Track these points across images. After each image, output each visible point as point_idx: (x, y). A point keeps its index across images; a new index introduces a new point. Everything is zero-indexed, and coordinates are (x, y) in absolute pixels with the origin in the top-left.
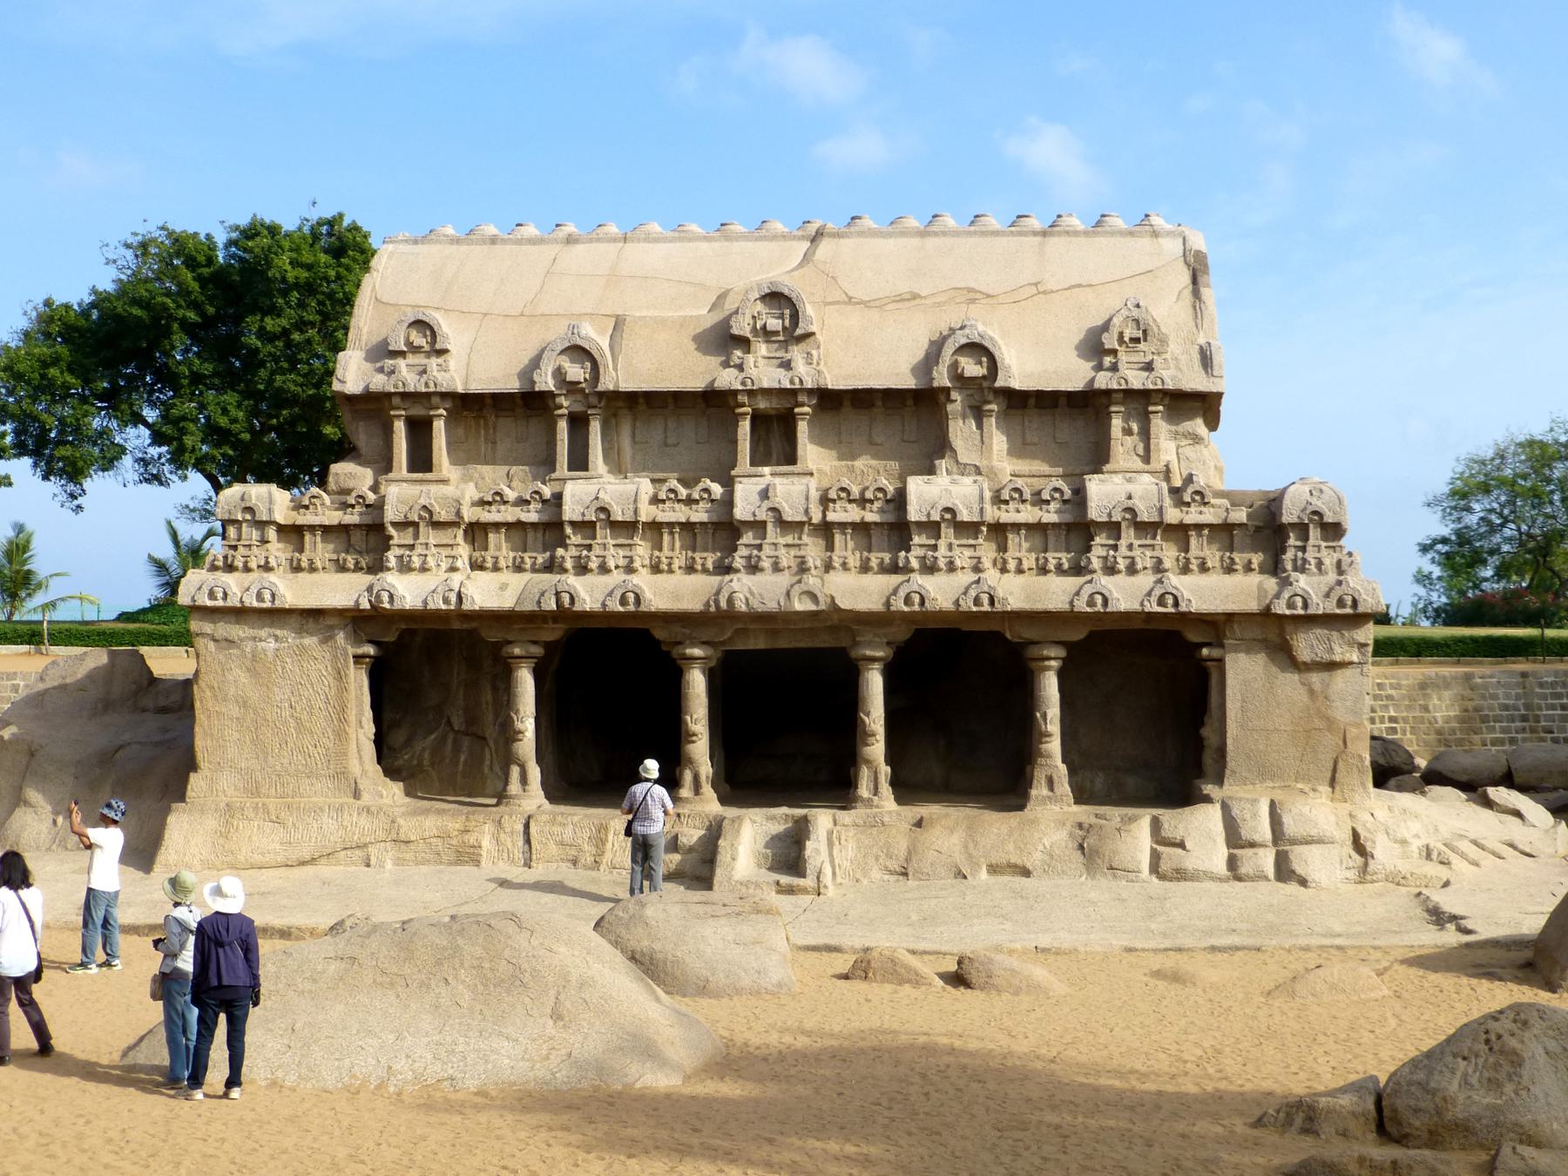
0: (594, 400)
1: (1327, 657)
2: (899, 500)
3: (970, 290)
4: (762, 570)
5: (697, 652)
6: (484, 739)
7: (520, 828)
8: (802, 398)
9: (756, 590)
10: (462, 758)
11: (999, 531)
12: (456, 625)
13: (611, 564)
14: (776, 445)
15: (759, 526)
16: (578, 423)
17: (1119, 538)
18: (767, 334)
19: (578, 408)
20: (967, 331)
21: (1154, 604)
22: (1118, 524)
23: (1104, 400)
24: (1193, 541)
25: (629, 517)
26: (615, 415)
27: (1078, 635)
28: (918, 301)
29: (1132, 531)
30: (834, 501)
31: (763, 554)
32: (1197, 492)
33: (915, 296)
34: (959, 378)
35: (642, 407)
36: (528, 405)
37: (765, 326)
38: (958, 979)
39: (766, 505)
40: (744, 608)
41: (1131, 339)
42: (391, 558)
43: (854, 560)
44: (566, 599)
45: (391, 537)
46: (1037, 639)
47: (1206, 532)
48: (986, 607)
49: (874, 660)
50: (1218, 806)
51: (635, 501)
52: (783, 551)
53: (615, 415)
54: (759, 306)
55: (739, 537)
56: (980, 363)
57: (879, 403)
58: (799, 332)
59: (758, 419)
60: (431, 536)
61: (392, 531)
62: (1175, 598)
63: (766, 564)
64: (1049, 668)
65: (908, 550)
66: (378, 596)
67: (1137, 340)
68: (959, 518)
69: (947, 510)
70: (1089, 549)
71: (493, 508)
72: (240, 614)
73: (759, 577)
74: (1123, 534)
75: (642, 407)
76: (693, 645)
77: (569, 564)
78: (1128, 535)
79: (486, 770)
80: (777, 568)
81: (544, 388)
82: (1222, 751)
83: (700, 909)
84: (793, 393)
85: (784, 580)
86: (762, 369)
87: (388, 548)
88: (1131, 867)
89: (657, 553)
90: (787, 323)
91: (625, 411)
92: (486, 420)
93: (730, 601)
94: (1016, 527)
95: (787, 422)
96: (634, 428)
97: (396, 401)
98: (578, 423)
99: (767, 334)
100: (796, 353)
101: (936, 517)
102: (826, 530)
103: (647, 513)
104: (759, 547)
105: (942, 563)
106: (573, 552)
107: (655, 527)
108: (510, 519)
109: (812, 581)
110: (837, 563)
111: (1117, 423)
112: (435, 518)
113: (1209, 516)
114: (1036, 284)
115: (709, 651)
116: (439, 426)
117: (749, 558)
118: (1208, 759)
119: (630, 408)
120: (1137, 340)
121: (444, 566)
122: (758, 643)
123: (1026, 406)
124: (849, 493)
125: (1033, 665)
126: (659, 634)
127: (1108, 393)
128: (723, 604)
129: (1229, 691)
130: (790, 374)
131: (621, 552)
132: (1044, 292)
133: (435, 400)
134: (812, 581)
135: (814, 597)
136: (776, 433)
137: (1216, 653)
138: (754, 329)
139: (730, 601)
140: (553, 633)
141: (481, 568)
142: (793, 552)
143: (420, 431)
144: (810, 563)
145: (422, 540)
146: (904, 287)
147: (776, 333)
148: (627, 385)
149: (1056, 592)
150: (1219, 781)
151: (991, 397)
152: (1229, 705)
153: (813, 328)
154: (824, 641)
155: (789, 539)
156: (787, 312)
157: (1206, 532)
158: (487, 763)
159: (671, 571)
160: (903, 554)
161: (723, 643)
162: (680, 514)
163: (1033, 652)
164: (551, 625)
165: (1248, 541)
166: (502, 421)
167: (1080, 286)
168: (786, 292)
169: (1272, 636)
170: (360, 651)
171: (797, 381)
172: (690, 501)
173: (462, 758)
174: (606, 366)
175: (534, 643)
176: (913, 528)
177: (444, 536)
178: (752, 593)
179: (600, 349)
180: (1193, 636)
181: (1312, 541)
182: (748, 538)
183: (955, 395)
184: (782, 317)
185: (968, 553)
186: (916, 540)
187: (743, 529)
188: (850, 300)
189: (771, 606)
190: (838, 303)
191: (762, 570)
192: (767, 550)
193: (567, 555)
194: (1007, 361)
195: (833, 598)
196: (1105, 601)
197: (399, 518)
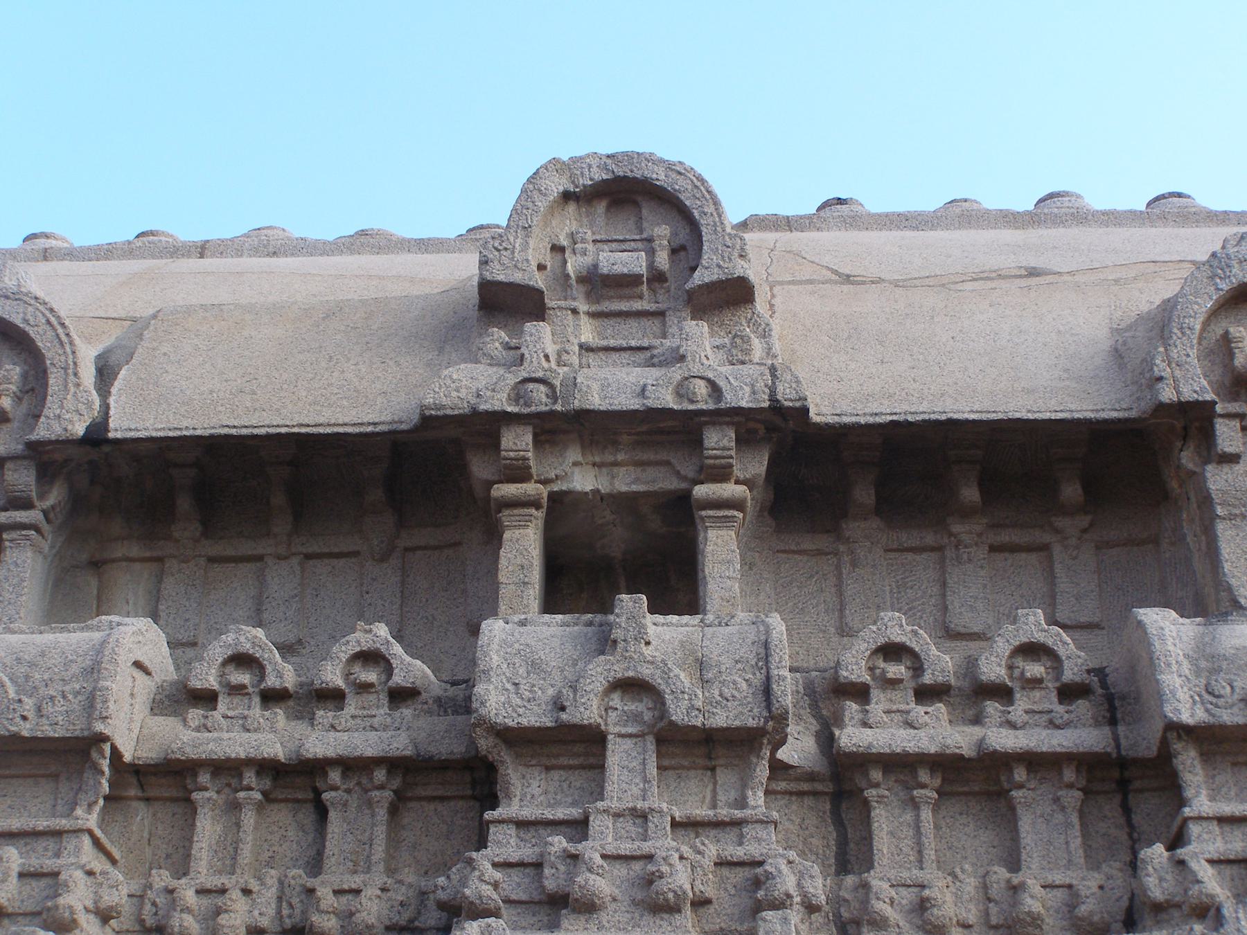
2: (1114, 693)
4: (588, 907)
8: (719, 440)
15: (571, 746)
26: (97, 565)
30: (860, 693)
31: (591, 850)
33: (1033, 273)
52: (663, 843)
57: (970, 494)
58: (701, 277)
65: (1177, 841)
89: (162, 878)
90: (663, 260)
102: (842, 788)
103: (134, 729)
104: (579, 827)
107: (166, 783)
124: (918, 668)
130: (676, 373)
136: (626, 558)
168: (660, 176)
171: (701, 388)
182: (528, 793)
191: (588, 907)
192: (607, 835)
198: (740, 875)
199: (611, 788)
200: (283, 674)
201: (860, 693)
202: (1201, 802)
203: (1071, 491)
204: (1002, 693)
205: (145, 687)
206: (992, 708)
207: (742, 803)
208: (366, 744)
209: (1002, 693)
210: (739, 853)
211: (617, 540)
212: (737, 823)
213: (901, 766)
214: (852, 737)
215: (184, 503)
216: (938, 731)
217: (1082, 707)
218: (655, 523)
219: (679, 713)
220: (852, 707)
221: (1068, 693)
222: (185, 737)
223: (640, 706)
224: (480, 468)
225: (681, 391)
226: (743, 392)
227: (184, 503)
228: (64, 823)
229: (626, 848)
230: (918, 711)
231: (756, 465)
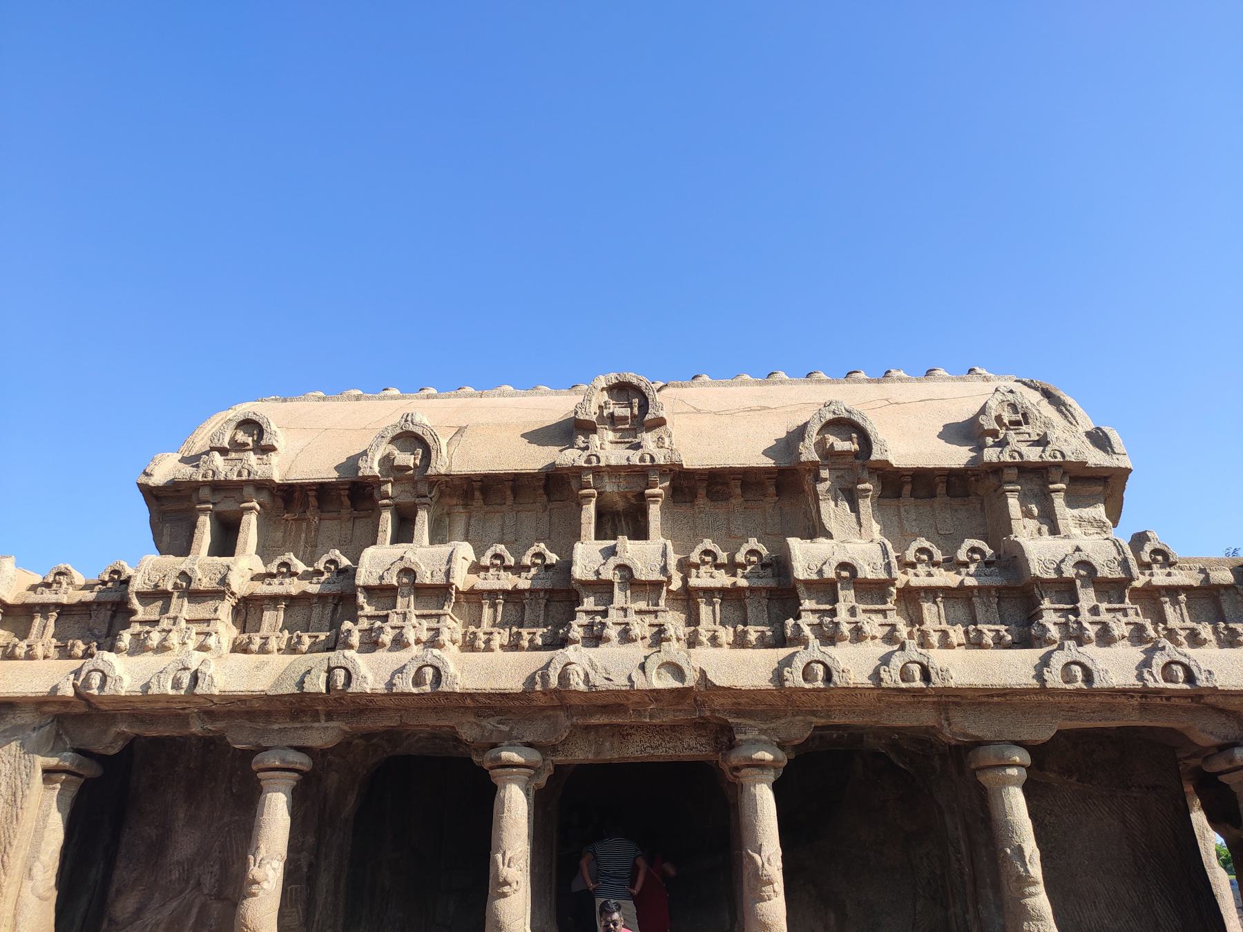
0: (424, 489)
2: (780, 565)
4: (608, 640)
9: (604, 664)
11: (911, 598)
12: (196, 728)
13: (410, 636)
15: (602, 589)
18: (613, 420)
19: (406, 499)
20: (832, 407)
21: (1159, 678)
22: (1070, 583)
23: (993, 480)
25: (439, 579)
27: (1043, 733)
29: (1091, 592)
30: (697, 567)
31: (608, 621)
32: (1156, 552)
33: (764, 408)
34: (829, 455)
37: (612, 414)
39: (613, 561)
40: (582, 687)
41: (1012, 423)
42: (126, 638)
43: (726, 635)
44: (340, 676)
45: (134, 612)
46: (988, 735)
47: (1182, 597)
48: (918, 684)
49: (761, 765)
51: (449, 561)
52: (633, 618)
54: (605, 396)
55: (579, 602)
56: (851, 439)
60: (184, 609)
61: (135, 603)
62: (1187, 669)
63: (612, 632)
64: (1009, 781)
65: (798, 617)
67: (1018, 423)
68: (860, 575)
69: (843, 566)
71: (276, 581)
73: (603, 648)
76: (511, 747)
77: (355, 639)
80: (626, 637)
81: (368, 473)
85: (638, 651)
86: (608, 449)
87: (127, 625)
89: (472, 629)
90: (636, 411)
93: (564, 677)
94: (932, 592)
96: (468, 525)
97: (205, 493)
99: (613, 420)
100: (648, 440)
101: (830, 573)
103: (462, 579)
104: (605, 614)
105: (845, 629)
106: (364, 623)
107: (474, 597)
108: (294, 591)
109: (674, 650)
110: (704, 637)
111: (1013, 503)
112: (193, 586)
113: (1180, 578)
115: (535, 756)
117: (589, 627)
119: (465, 505)
120: (1018, 423)
121: (191, 644)
124: (715, 557)
125: (986, 778)
126: (468, 732)
128: (554, 682)
130: (640, 452)
131: (425, 623)
133: (248, 491)
134: (674, 650)
135: (677, 671)
138: (601, 416)
139: (564, 677)
140: (323, 735)
141: (245, 651)
142: (649, 619)
144: (671, 632)
145: (172, 613)
147: (623, 419)
148: (461, 466)
149: (1011, 668)
151: (865, 475)
153: (663, 414)
154: (691, 748)
155: (642, 605)
156: (636, 401)
157: (1182, 597)
159: (488, 649)
160: (791, 621)
161: (554, 749)
162: (508, 581)
163: (987, 755)
164: (323, 724)
166: (327, 523)
170: (53, 761)
171: (648, 458)
172: (518, 569)
174: (439, 451)
175: (299, 749)
176: (801, 590)
177: (202, 610)
178: (592, 665)
182: (589, 603)
183: (825, 473)
184: (631, 406)
185: (878, 619)
186: (807, 604)
187: (582, 593)
188: (699, 411)
189: (620, 682)
191: (608, 640)
192: (614, 615)
193: (354, 631)
194: (880, 437)
195: (703, 673)
197: (148, 588)
198: (656, 629)
199: (616, 600)
200: (510, 561)
205: (467, 565)
207: (657, 605)
210: (656, 622)
211: (621, 505)
212: (655, 612)
214: (694, 582)
215: (477, 494)
217: (769, 571)
218: (633, 501)
220: (694, 571)
222: (480, 582)
223: (626, 573)
225: (642, 459)
227: (477, 494)
228: (441, 612)
230: (716, 572)
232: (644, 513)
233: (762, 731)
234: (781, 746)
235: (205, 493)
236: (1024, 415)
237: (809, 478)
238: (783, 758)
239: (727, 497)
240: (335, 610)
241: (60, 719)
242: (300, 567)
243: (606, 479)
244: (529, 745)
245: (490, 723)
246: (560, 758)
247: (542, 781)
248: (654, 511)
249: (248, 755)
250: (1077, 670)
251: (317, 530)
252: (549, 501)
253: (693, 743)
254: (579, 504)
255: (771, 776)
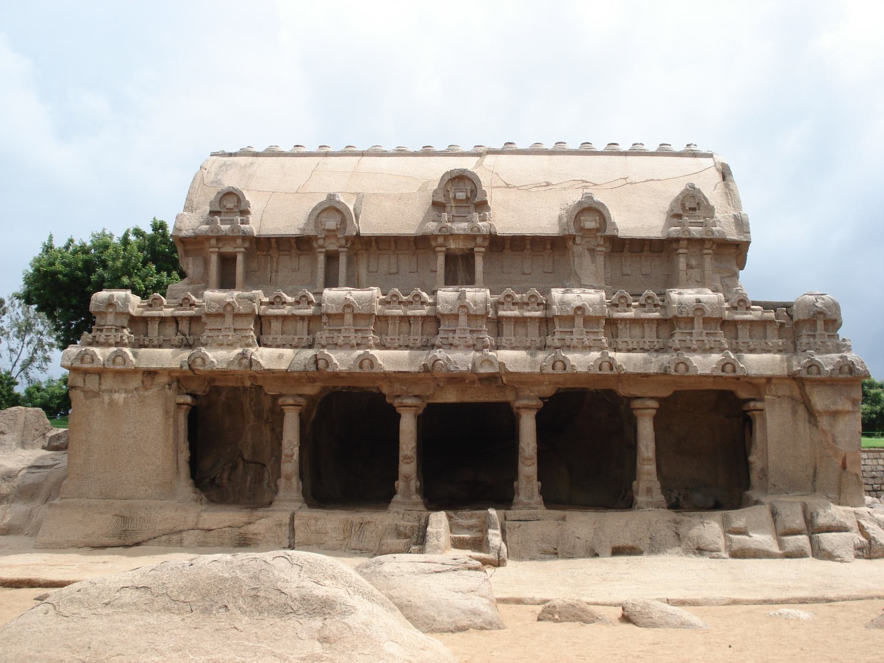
0: (343, 242)
1: (833, 408)
3: (583, 181)
5: (409, 401)
6: (264, 466)
7: (287, 520)
8: (479, 241)
10: (249, 478)
14: (461, 274)
16: (332, 258)
17: (693, 328)
23: (675, 246)
24: (740, 333)
26: (356, 254)
27: (665, 393)
28: (550, 187)
29: (701, 325)
30: (503, 304)
33: (548, 184)
35: (374, 248)
36: (301, 244)
38: (626, 619)
41: (690, 209)
44: (321, 364)
45: (205, 324)
46: (639, 394)
50: (768, 506)
53: (356, 254)
57: (528, 247)
58: (477, 200)
59: (450, 258)
62: (734, 366)
66: (194, 362)
67: (694, 209)
68: (587, 314)
70: (672, 335)
72: (100, 373)
74: (696, 326)
75: (374, 248)
76: (408, 397)
78: (698, 325)
79: (265, 486)
82: (764, 472)
83: (426, 566)
84: (474, 237)
88: (711, 547)
90: (469, 194)
91: (363, 252)
92: (271, 257)
95: (468, 258)
96: (368, 262)
98: (332, 258)
111: (682, 262)
112: (236, 311)
114: (625, 179)
116: (240, 258)
118: (754, 477)
119: (366, 250)
120: (694, 209)
122: (450, 397)
123: (623, 248)
124: (513, 299)
125: (636, 413)
127: (677, 240)
129: (769, 431)
132: (631, 183)
137: (759, 405)
140: (311, 390)
143: (227, 262)
146: (542, 179)
150: (765, 490)
152: (769, 440)
154: (493, 397)
158: (266, 482)
161: (428, 397)
163: (637, 404)
165: (776, 332)
167: (653, 180)
168: (469, 175)
169: (796, 393)
173: (249, 478)
175: (300, 395)
176: (556, 320)
179: (347, 209)
180: (743, 394)
181: (818, 332)
188: (508, 186)
190: (500, 187)
196: (687, 369)
201: (503, 304)
202: (558, 329)
203: (548, 246)
204: (527, 304)
206: (525, 306)
208: (418, 312)
209: (527, 304)
213: (509, 318)
214: (501, 313)
215: (374, 243)
216: (516, 313)
219: (471, 312)
221: (539, 304)
223: (465, 310)
224: (433, 244)
226: (485, 231)
227: (374, 243)
229: (462, 336)
231: (487, 244)
232: (473, 257)
233: (531, 392)
234: (541, 398)
235: (213, 242)
236: (698, 204)
237: (571, 243)
238: (540, 404)
239: (523, 249)
240: (309, 325)
241: (178, 380)
242: (290, 299)
243: (451, 241)
244: (416, 396)
245: (397, 386)
246: (431, 401)
247: (421, 411)
248: (479, 262)
249: (275, 398)
250: (682, 366)
251: (277, 263)
252: (417, 248)
253: (497, 395)
254: (435, 253)
255: (533, 413)
